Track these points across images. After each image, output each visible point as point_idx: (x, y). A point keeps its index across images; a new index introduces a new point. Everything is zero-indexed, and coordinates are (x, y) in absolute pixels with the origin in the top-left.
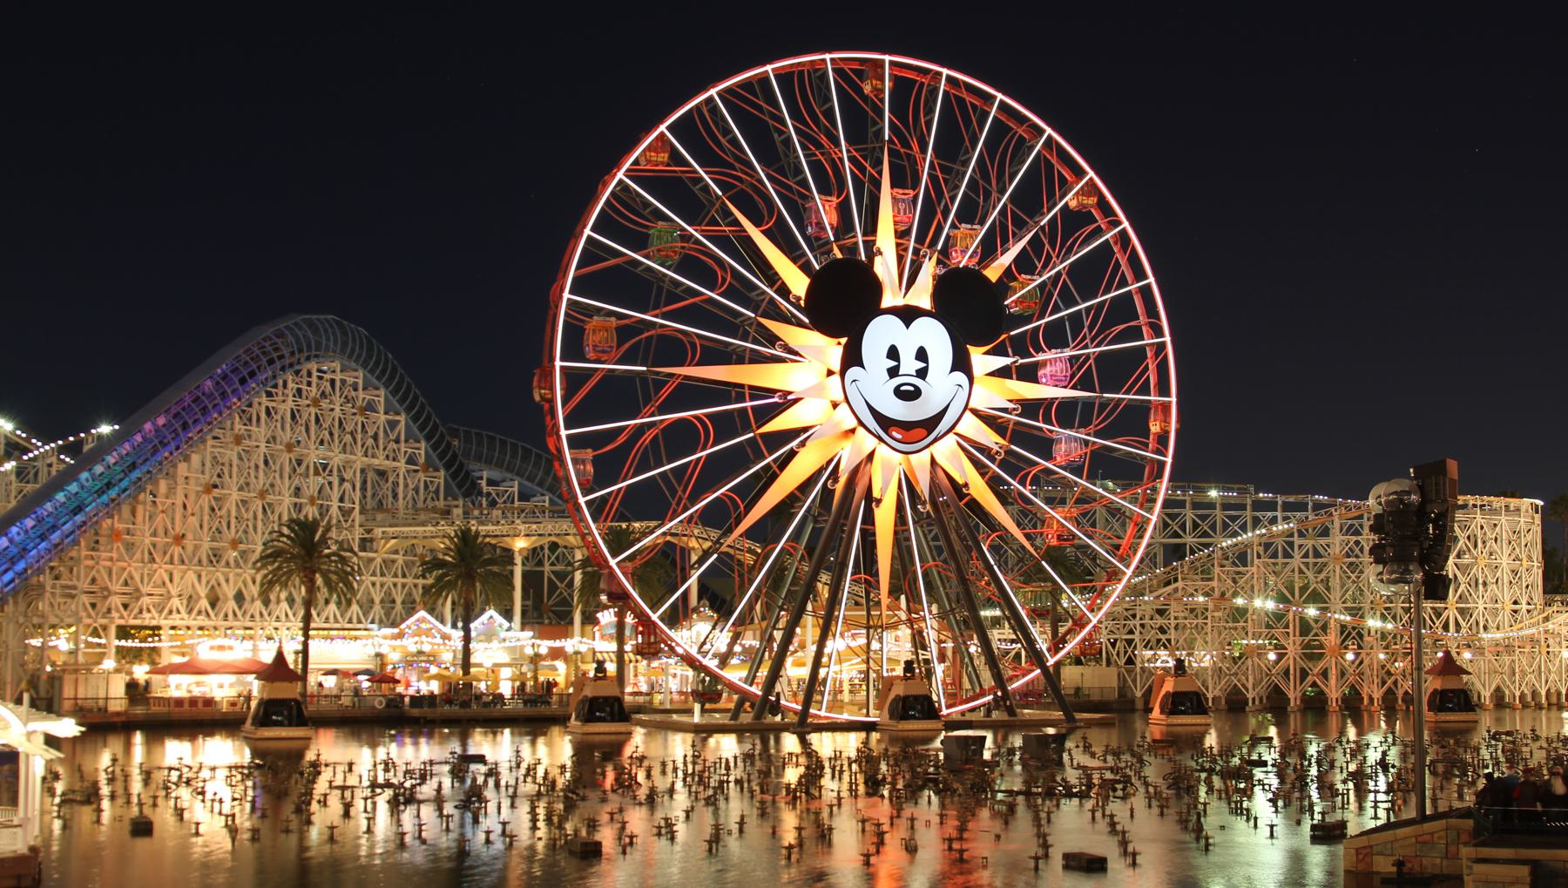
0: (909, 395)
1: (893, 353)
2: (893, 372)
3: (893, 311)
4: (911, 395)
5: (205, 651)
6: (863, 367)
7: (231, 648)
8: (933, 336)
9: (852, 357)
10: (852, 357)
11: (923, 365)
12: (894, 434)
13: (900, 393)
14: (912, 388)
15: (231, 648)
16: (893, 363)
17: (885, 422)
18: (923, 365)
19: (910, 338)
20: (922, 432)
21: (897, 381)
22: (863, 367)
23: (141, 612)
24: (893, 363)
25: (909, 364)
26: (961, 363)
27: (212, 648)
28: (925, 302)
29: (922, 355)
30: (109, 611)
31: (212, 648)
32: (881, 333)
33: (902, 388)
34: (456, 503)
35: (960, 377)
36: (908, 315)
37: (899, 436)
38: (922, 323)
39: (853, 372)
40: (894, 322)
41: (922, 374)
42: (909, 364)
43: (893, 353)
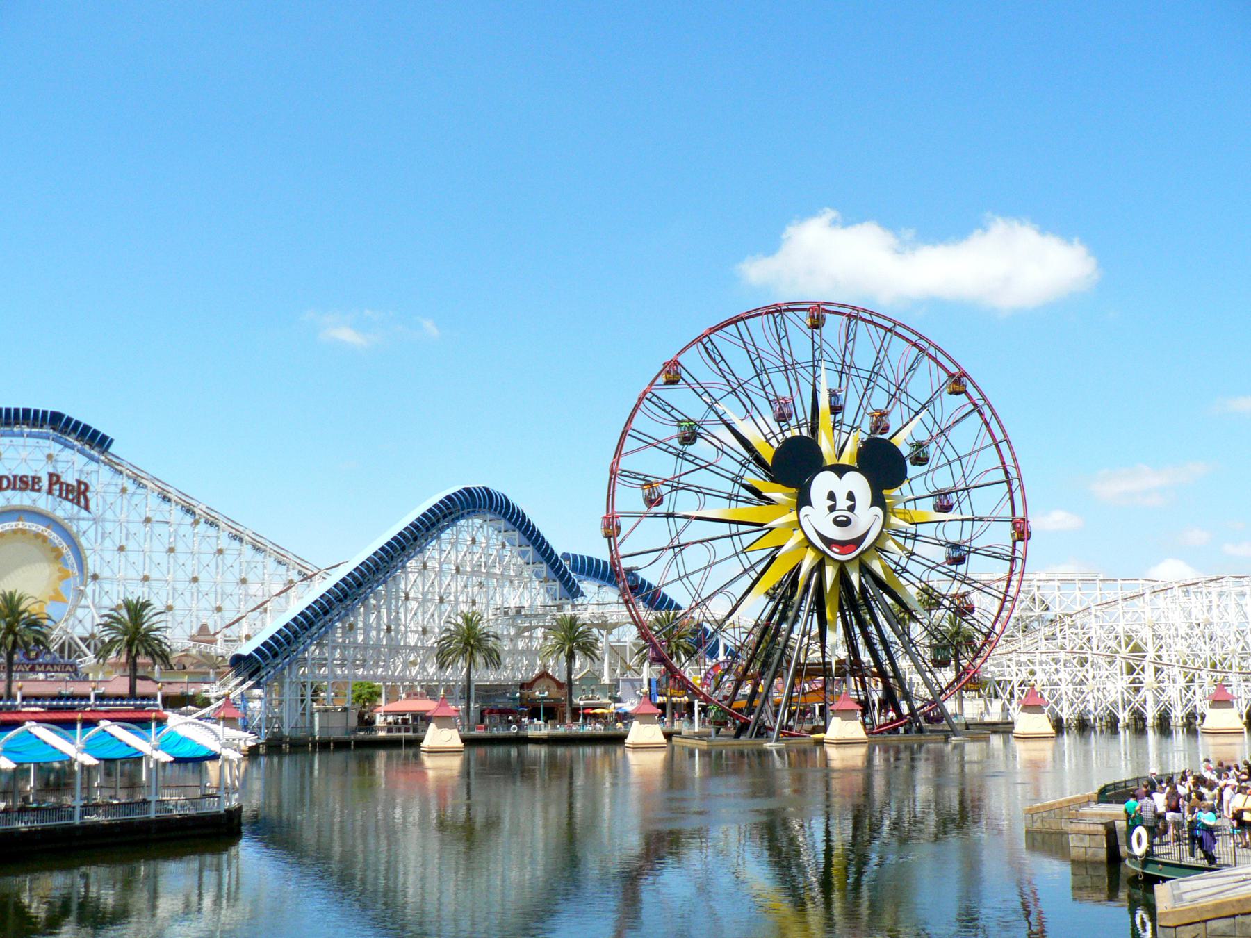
0: (843, 523)
1: (831, 496)
2: (832, 509)
4: (843, 523)
6: (811, 505)
8: (858, 483)
10: (804, 500)
11: (851, 503)
12: (834, 549)
13: (837, 522)
14: (845, 519)
17: (829, 542)
18: (851, 503)
20: (853, 547)
21: (835, 514)
22: (811, 505)
25: (843, 503)
29: (851, 496)
32: (823, 483)
33: (839, 519)
34: (568, 601)
35: (877, 510)
36: (840, 470)
37: (837, 550)
39: (805, 510)
41: (851, 509)
42: (843, 503)
43: (831, 496)
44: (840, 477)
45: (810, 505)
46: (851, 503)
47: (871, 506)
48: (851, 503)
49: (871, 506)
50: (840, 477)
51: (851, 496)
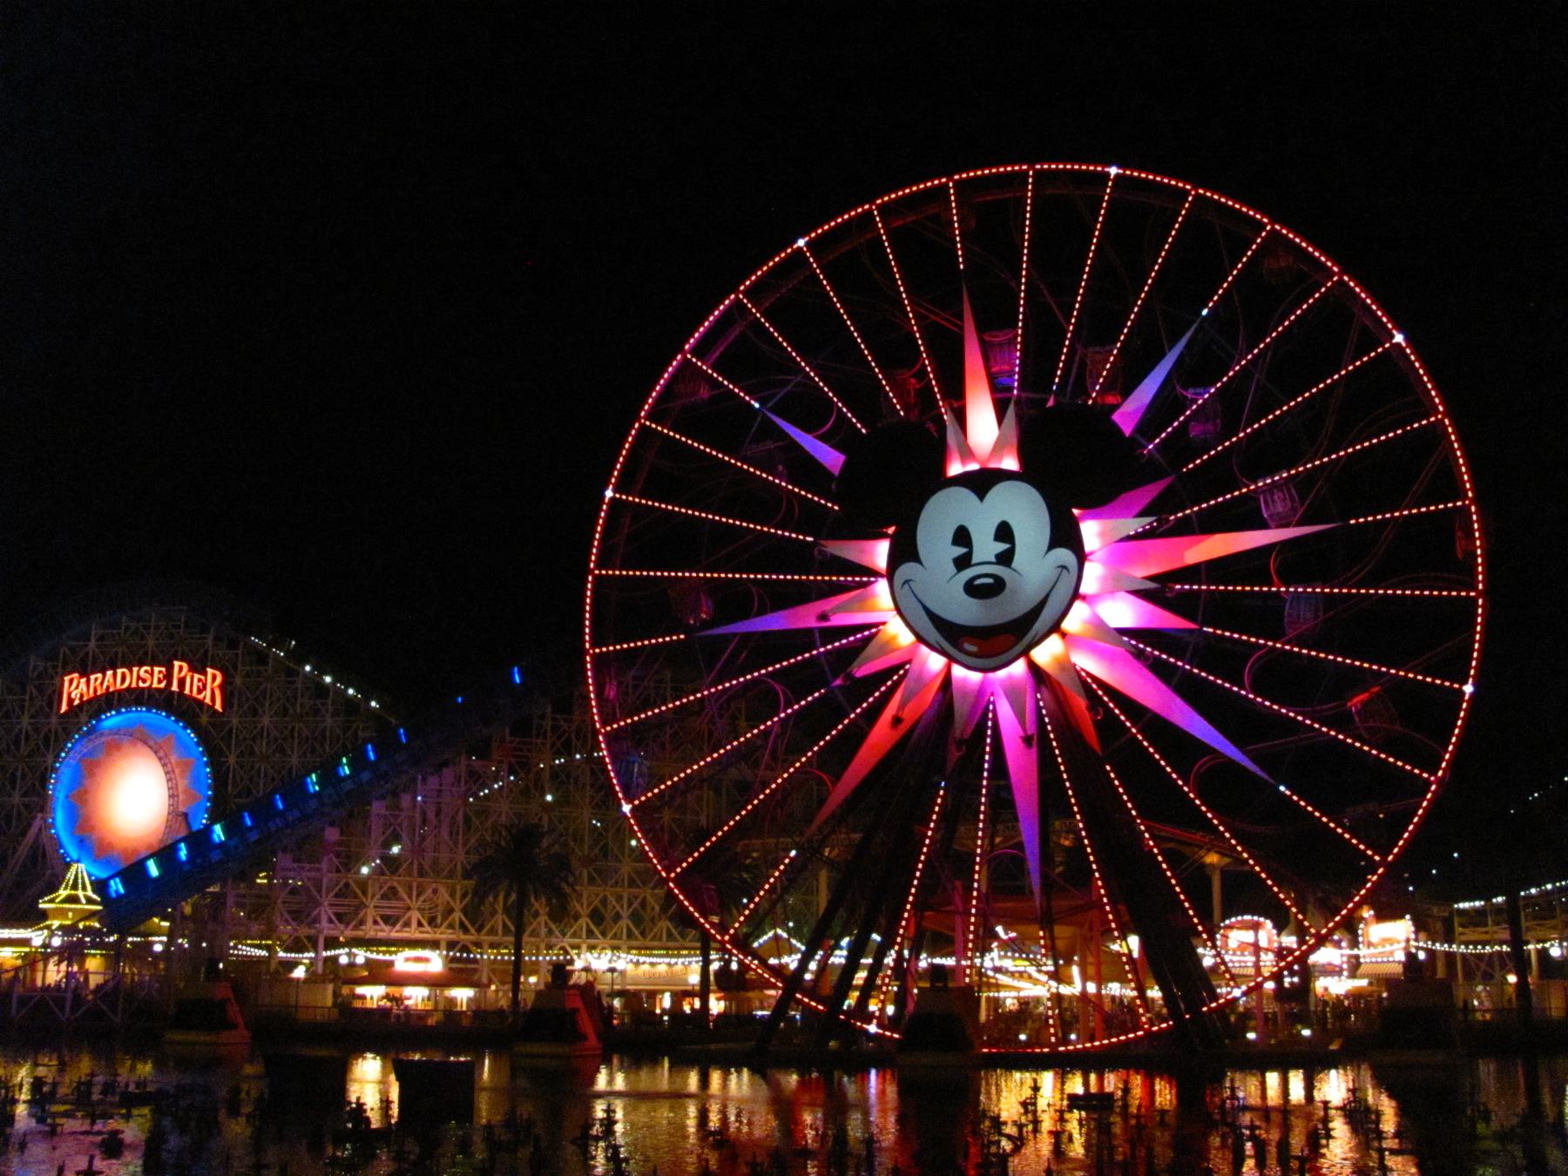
1: (962, 537)
2: (962, 563)
3: (964, 480)
4: (993, 589)
5: (402, 962)
6: (917, 559)
7: (427, 960)
9: (904, 552)
10: (904, 552)
13: (971, 589)
14: (990, 581)
15: (427, 960)
16: (961, 551)
19: (982, 517)
21: (968, 574)
23: (362, 922)
24: (961, 551)
25: (986, 548)
26: (1065, 535)
27: (407, 960)
28: (1010, 463)
29: (1004, 532)
30: (317, 920)
31: (407, 960)
33: (978, 582)
35: (1064, 555)
36: (982, 482)
38: (999, 492)
39: (907, 570)
40: (964, 495)
41: (1005, 559)
42: (986, 548)
44: (981, 495)
45: (917, 559)
46: (1002, 547)
47: (1053, 545)
48: (1002, 547)
49: (1053, 545)
50: (981, 496)
51: (1004, 532)
